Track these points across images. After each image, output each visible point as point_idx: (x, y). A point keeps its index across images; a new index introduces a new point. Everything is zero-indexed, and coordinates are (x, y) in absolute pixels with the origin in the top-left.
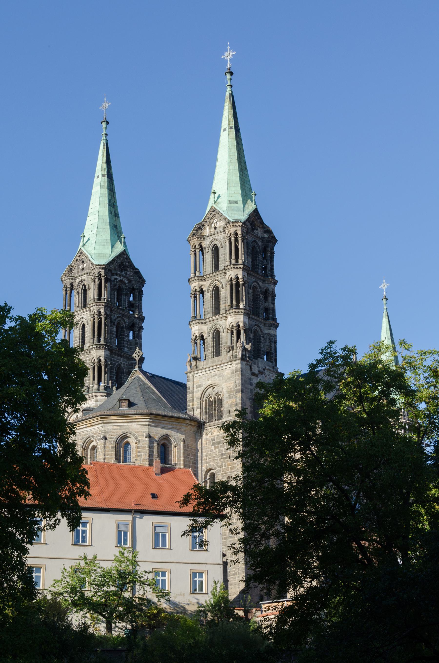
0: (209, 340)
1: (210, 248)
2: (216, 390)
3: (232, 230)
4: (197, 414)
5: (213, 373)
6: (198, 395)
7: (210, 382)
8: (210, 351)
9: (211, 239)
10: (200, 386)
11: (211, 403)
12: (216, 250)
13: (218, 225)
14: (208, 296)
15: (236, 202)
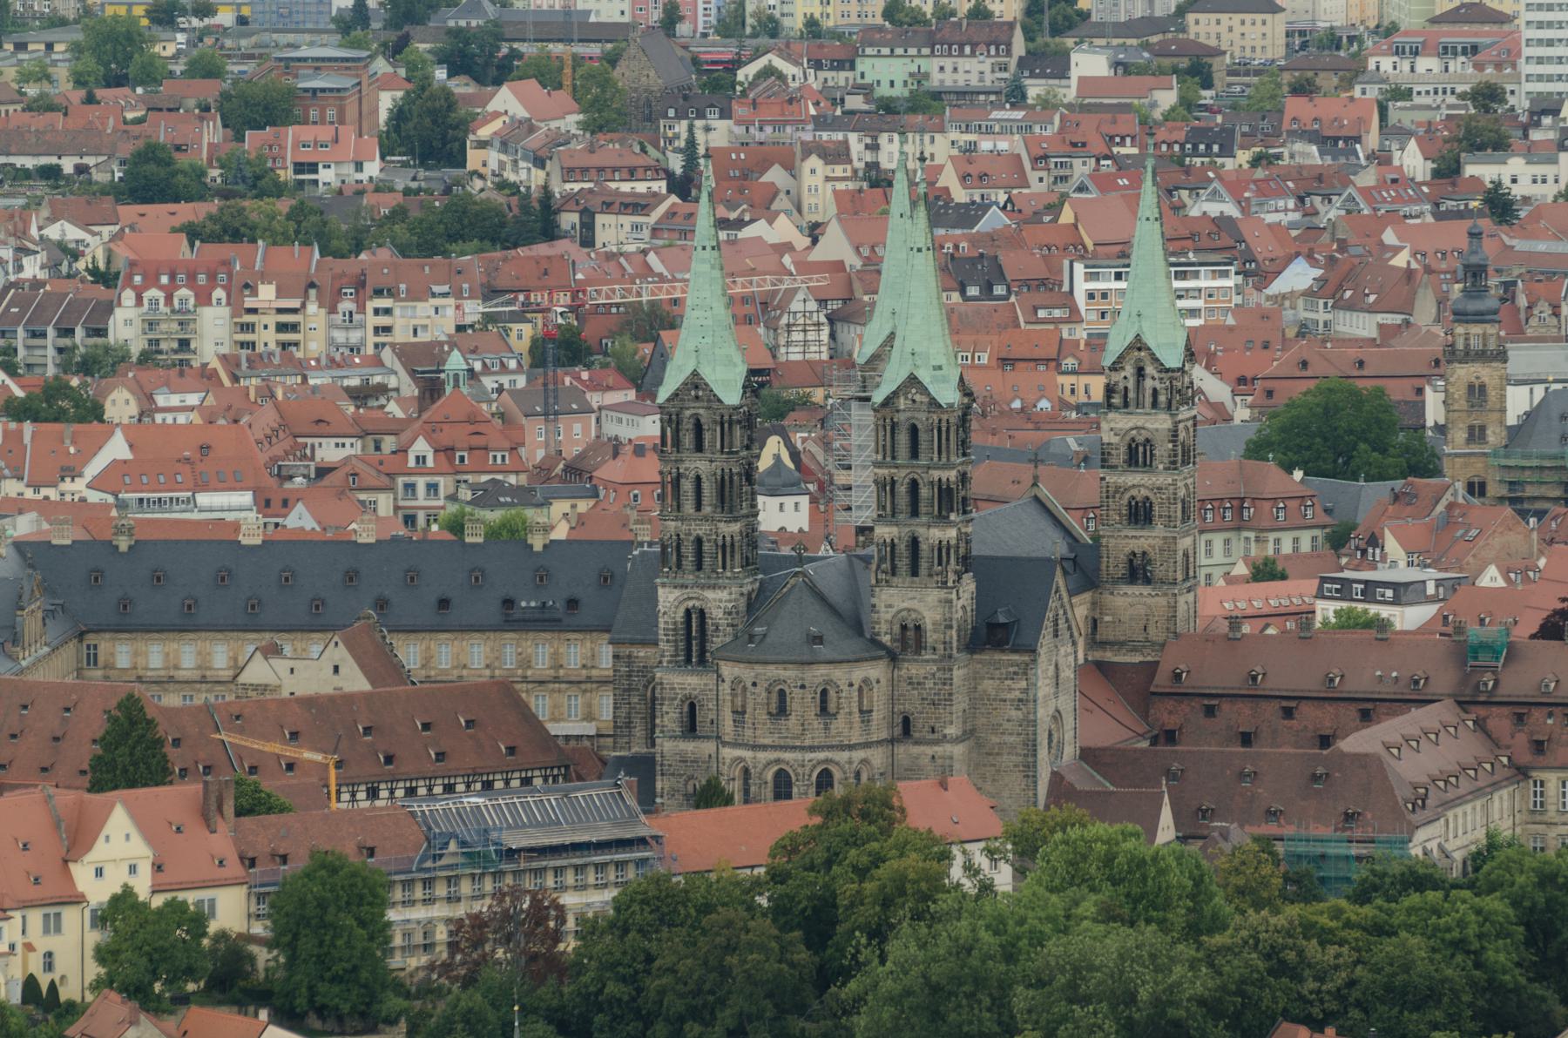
0: (902, 548)
1: (907, 425)
2: (914, 616)
3: (945, 417)
4: (886, 639)
5: (911, 595)
6: (889, 616)
7: (905, 605)
8: (903, 564)
9: (909, 414)
10: (890, 606)
11: (904, 628)
12: (914, 430)
13: (918, 398)
14: (902, 490)
15: (940, 368)
